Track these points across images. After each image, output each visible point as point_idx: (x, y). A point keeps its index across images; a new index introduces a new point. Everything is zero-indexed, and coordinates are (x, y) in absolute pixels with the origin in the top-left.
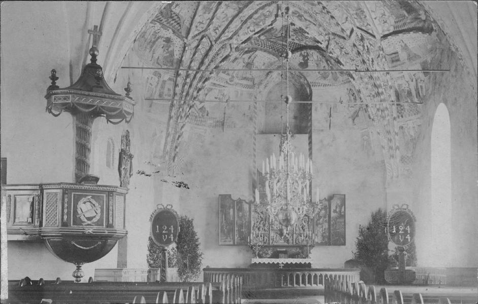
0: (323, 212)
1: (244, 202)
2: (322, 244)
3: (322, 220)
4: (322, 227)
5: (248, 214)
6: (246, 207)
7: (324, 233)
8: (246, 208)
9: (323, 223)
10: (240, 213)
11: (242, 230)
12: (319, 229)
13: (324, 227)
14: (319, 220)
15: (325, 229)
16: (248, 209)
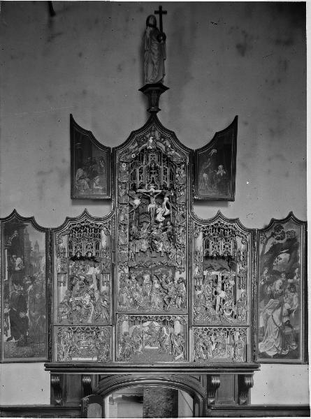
0: (284, 256)
1: (30, 225)
2: (279, 358)
3: (279, 282)
4: (281, 305)
5: (43, 261)
6: (37, 241)
7: (288, 324)
8: (37, 246)
9: (282, 294)
10: (18, 261)
11: (22, 315)
12: (269, 312)
13: (287, 306)
14: (270, 283)
15: (290, 312)
16: (42, 248)
